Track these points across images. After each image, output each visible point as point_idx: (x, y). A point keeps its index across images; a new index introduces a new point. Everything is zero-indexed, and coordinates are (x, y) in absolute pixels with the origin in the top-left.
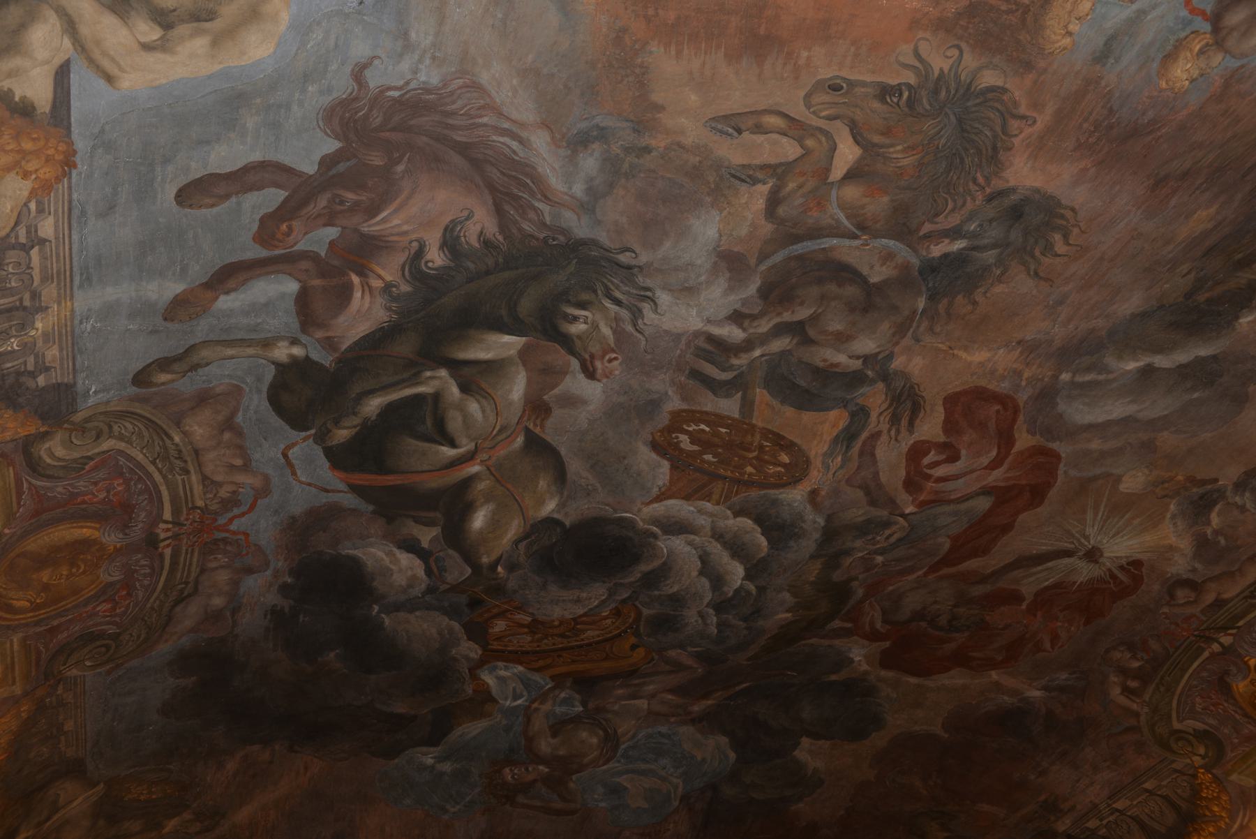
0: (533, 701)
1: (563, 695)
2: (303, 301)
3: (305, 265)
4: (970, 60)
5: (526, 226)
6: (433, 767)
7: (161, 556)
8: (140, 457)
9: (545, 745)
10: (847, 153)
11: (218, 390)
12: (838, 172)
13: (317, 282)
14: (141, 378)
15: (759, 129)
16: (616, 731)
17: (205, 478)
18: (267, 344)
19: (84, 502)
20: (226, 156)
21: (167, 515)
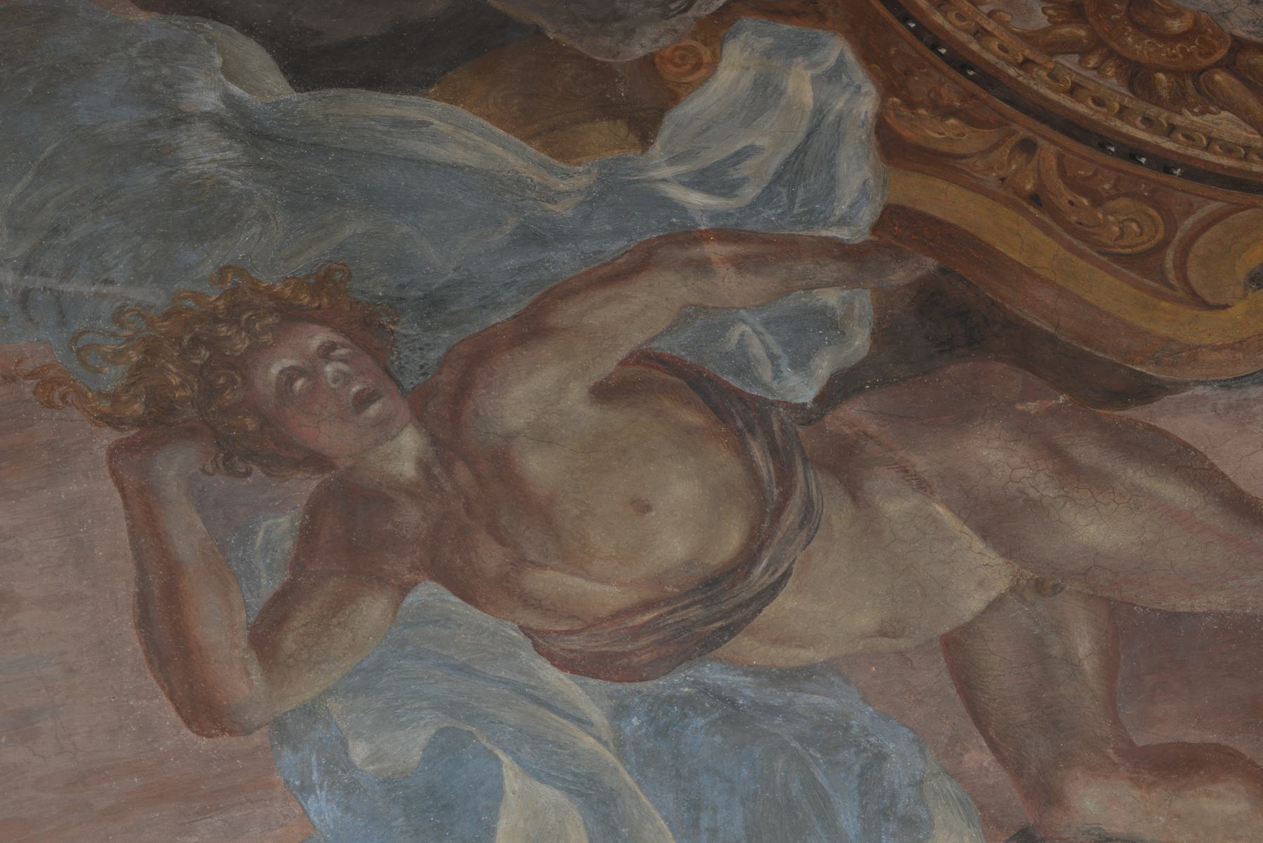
0: (722, 235)
1: (831, 298)
6: (180, 120)
9: (532, 397)
16: (773, 591)
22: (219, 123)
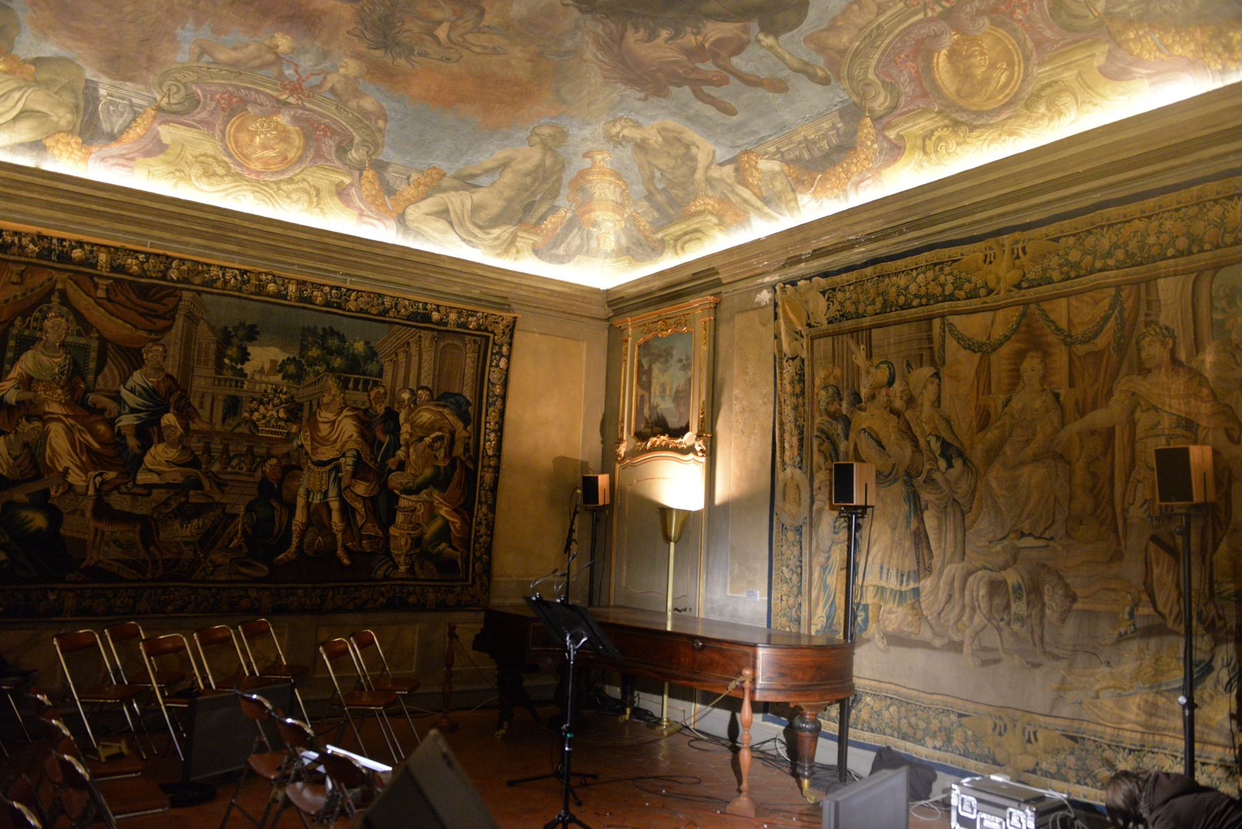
2: (738, 51)
3: (721, 63)
4: (389, 60)
5: (613, 26)
8: (877, 56)
10: (442, 32)
11: (812, 46)
12: (445, 26)
13: (723, 54)
14: (825, 82)
15: (484, 47)
17: (878, 14)
18: (770, 48)
19: (917, 72)
20: (710, 111)
21: (921, 16)
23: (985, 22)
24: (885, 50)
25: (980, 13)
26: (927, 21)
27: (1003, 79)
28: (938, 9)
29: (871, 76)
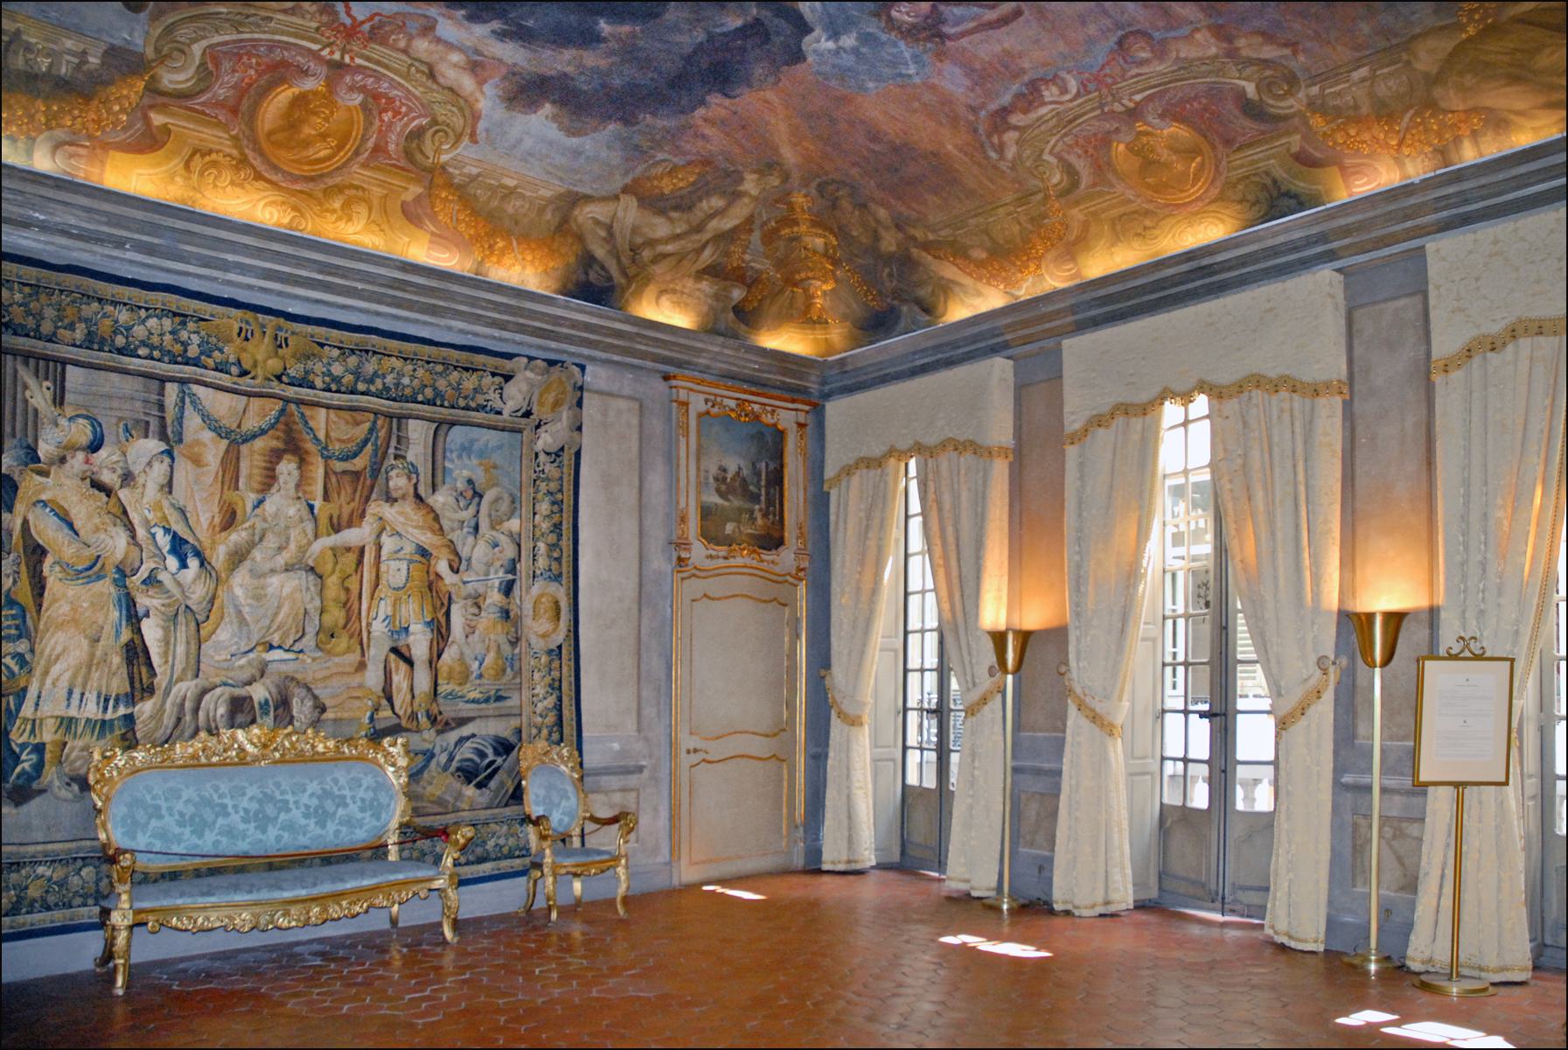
7: (359, 66)
8: (227, 38)
19: (250, 85)
21: (315, 47)
22: (836, 41)
23: (357, 99)
24: (242, 40)
25: (363, 89)
26: (315, 55)
27: (322, 154)
28: (337, 56)
29: (197, 49)
